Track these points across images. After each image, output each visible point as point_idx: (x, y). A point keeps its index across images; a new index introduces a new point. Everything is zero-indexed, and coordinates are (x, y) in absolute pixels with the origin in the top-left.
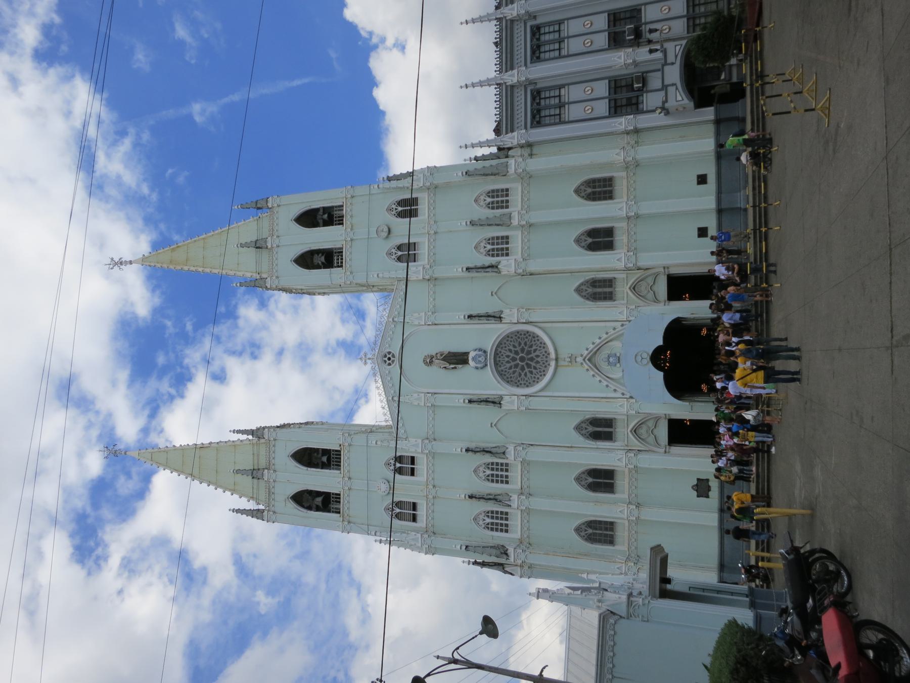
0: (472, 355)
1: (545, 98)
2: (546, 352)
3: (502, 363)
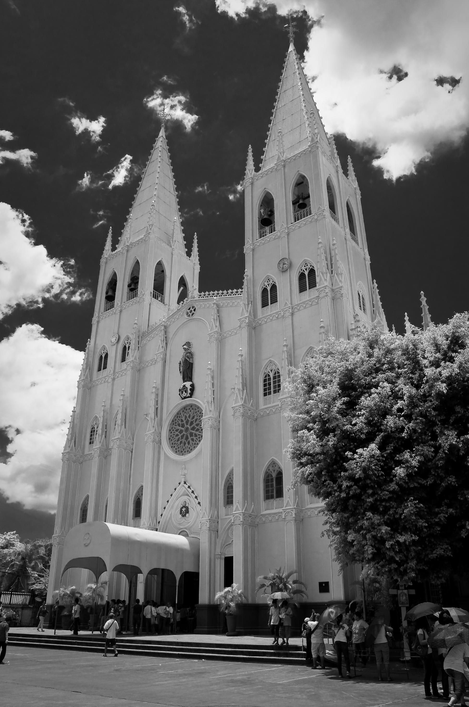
0: (188, 384)
2: (191, 450)
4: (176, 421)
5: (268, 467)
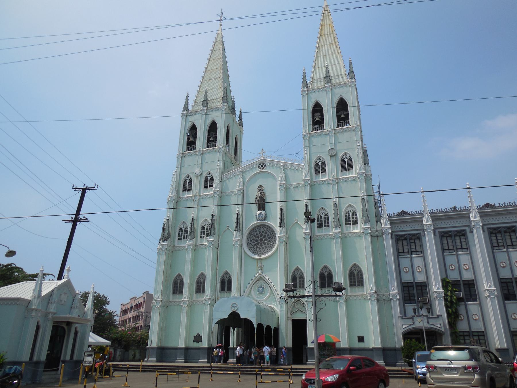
0: (263, 212)
1: (415, 242)
2: (265, 253)
3: (259, 229)
4: (252, 234)
5: (322, 269)
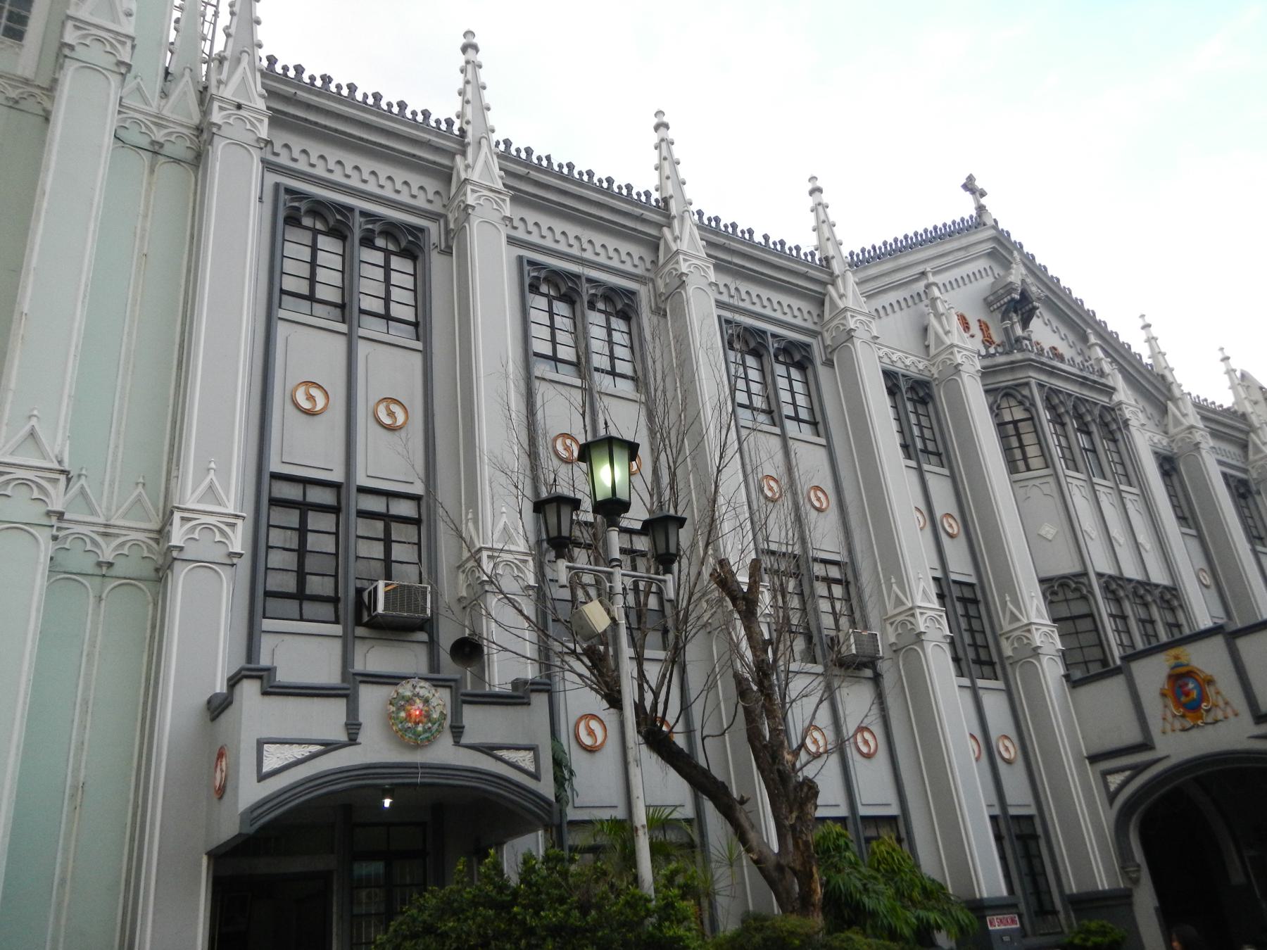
1: (387, 269)
